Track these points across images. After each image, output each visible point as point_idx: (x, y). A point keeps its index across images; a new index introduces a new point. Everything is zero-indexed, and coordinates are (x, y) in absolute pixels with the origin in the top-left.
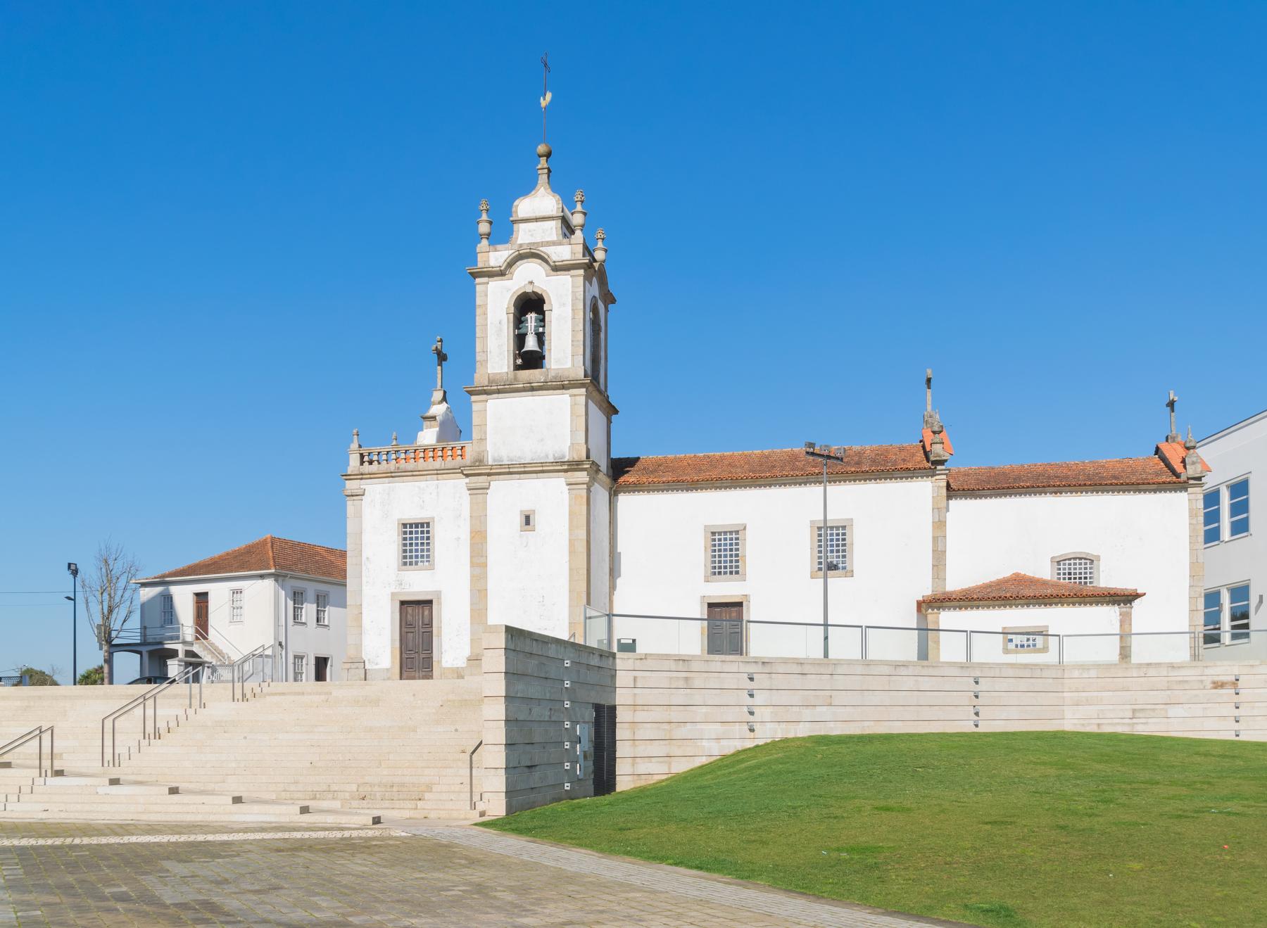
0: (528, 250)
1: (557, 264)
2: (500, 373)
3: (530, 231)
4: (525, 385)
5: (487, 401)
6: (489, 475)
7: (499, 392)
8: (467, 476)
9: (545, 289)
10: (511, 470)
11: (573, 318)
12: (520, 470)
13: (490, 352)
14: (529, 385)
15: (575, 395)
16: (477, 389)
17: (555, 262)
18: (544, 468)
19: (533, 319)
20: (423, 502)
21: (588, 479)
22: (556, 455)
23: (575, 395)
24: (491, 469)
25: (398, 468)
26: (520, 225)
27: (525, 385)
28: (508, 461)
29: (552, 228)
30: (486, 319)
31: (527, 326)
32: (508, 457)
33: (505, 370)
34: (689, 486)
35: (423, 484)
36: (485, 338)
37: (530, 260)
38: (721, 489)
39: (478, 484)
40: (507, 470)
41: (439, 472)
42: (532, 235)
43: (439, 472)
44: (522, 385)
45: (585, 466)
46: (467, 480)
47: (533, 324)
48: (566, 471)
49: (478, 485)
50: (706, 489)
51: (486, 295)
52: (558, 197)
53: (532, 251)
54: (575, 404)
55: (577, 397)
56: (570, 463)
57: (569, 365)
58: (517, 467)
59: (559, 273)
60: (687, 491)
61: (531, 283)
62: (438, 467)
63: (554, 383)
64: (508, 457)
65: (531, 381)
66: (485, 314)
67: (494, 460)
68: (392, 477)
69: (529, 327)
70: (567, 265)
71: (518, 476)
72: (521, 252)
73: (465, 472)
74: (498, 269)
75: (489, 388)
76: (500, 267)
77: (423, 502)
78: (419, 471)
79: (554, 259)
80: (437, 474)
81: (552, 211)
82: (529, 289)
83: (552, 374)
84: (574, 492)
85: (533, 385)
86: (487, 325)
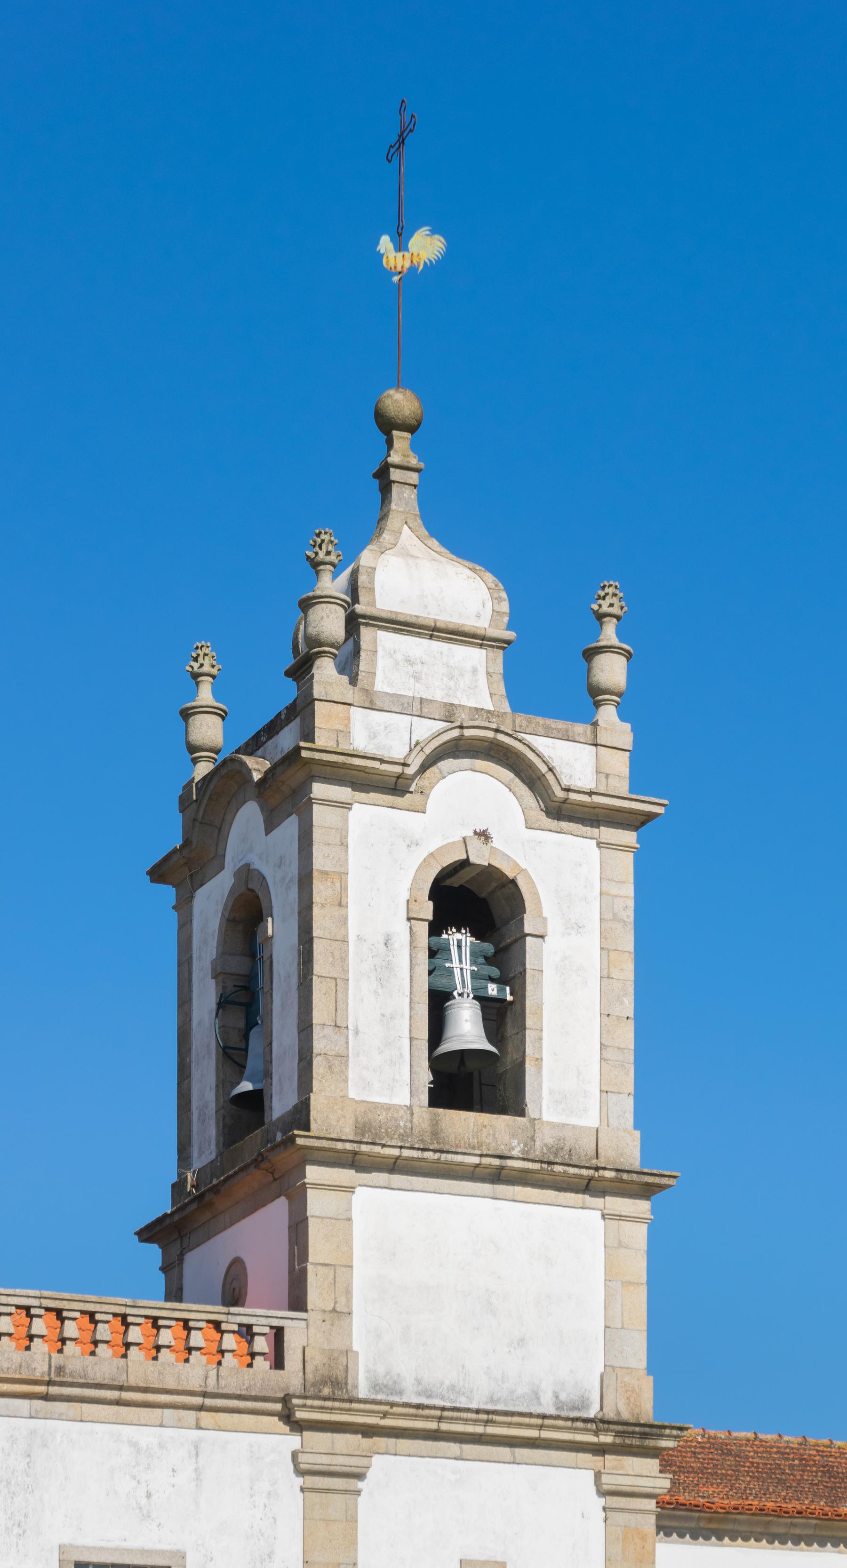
0: (490, 734)
1: (573, 796)
2: (388, 1108)
3: (409, 661)
4: (486, 1161)
5: (351, 1189)
6: (368, 1431)
7: (395, 1167)
8: (298, 1426)
9: (523, 865)
10: (444, 1426)
11: (606, 977)
12: (470, 1429)
13: (357, 1032)
14: (496, 1162)
15: (620, 1217)
16: (340, 1146)
17: (568, 790)
18: (546, 1434)
19: (466, 951)
20: (149, 1495)
21: (667, 1484)
22: (563, 1397)
23: (620, 1217)
24: (385, 1415)
25: (60, 1370)
26: (382, 635)
27: (486, 1161)
28: (419, 1394)
29: (475, 671)
30: (344, 921)
31: (450, 971)
32: (419, 1382)
33: (402, 1098)
34: (702, 1524)
35: (147, 1436)
36: (340, 982)
37: (480, 763)
38: (783, 1542)
39: (341, 1460)
40: (433, 1425)
41: (209, 1402)
42: (417, 678)
43: (209, 1402)
44: (476, 1160)
45: (664, 1443)
46: (294, 1441)
47: (468, 966)
48: (600, 1450)
49: (340, 1462)
50: (746, 1539)
51: (344, 845)
52: (489, 577)
53: (501, 737)
54: (620, 1245)
55: (626, 1226)
56: (602, 1423)
57: (591, 1119)
58: (466, 1421)
59: (564, 825)
60: (695, 1537)
61: (484, 835)
62: (195, 1384)
63: (572, 1170)
64: (419, 1382)
65: (503, 1150)
66: (341, 904)
67: (375, 1386)
68: (46, 1397)
69: (457, 973)
70: (595, 807)
71: (454, 1448)
72: (468, 733)
73: (300, 1415)
74: (398, 769)
75: (377, 1149)
76: (405, 765)
77: (149, 1495)
78: (145, 1390)
79: (565, 782)
80: (201, 1408)
81: (478, 616)
82: (479, 857)
83: (545, 1139)
84: (621, 1518)
85: (510, 1163)
86: (345, 941)
